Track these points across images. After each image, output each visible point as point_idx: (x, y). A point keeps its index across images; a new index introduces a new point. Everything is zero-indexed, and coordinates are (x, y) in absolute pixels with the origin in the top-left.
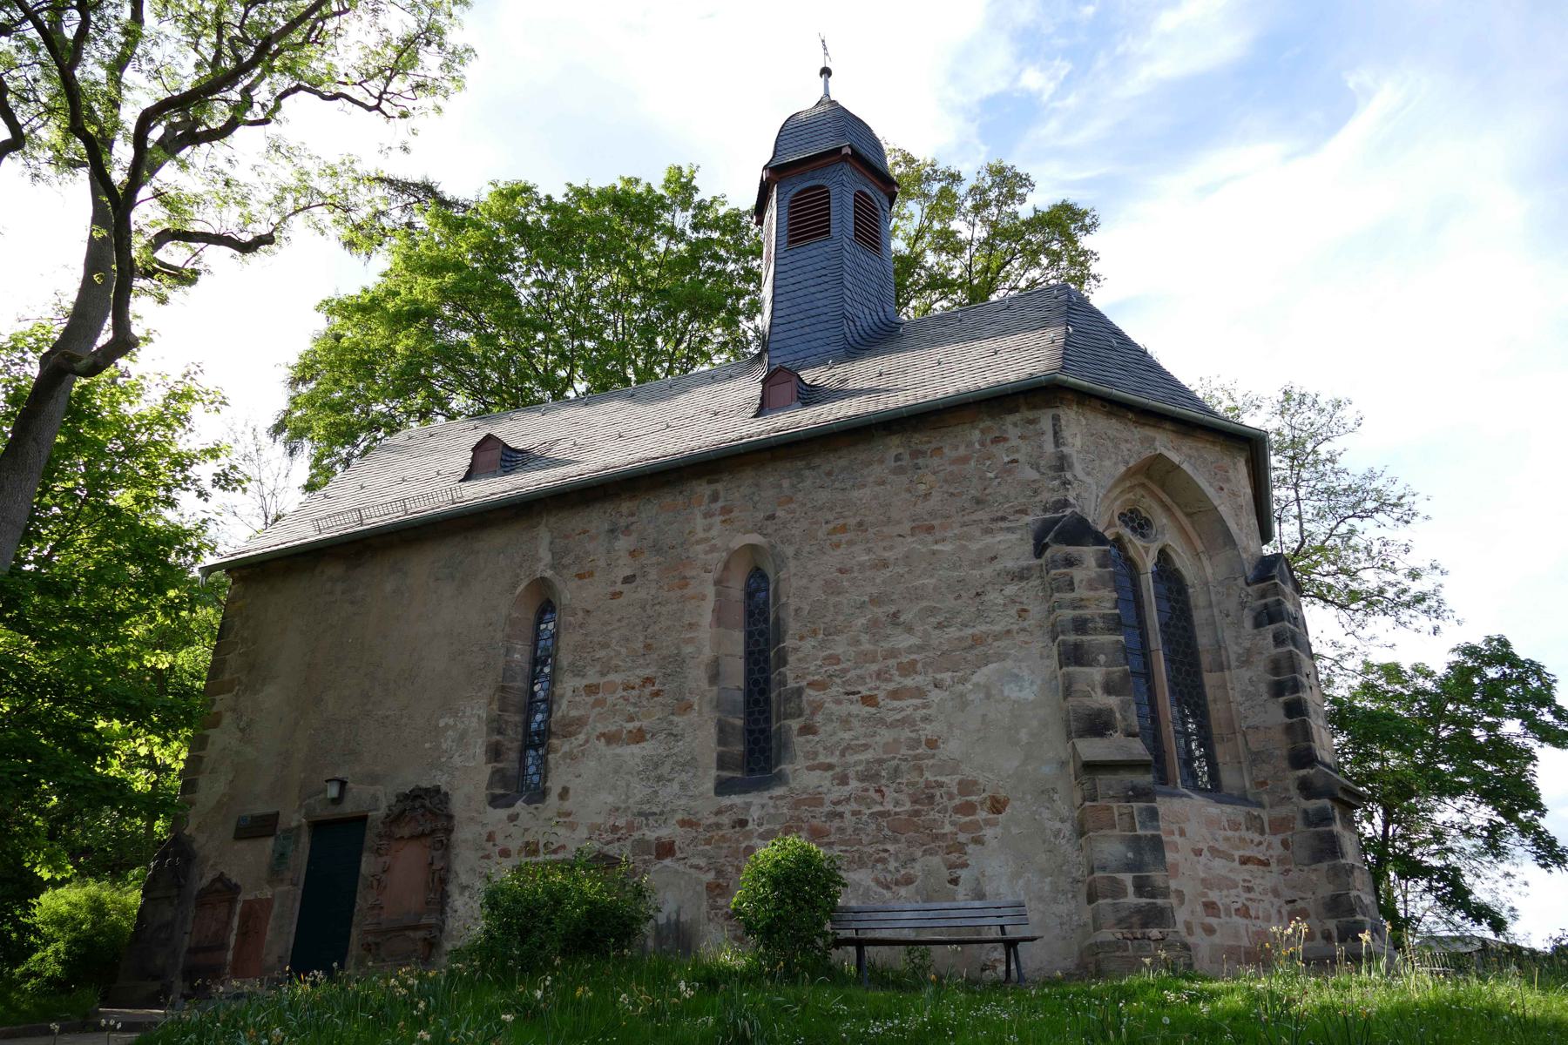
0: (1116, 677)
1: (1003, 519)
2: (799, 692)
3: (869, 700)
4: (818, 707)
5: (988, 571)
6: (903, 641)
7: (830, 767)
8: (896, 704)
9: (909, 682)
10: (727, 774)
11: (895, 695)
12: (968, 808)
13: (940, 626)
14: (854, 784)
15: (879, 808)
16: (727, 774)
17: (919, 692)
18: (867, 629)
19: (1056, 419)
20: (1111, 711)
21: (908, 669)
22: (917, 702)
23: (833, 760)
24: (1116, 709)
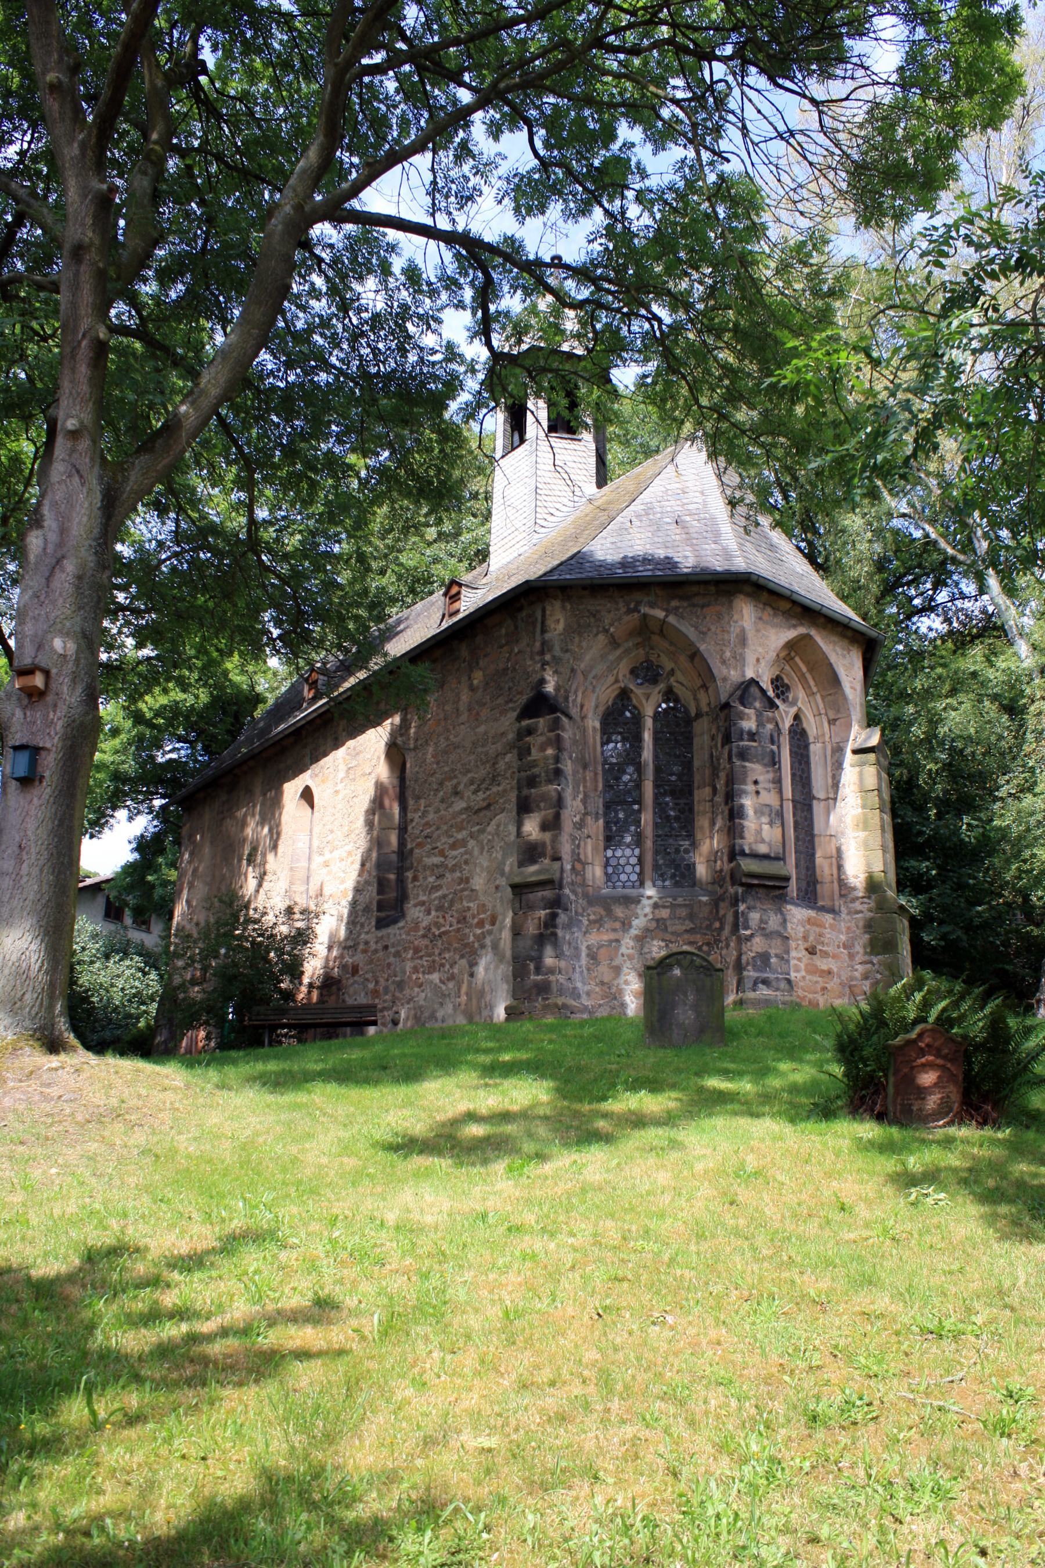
0: (550, 817)
1: (511, 701)
2: (412, 850)
3: (442, 853)
4: (420, 861)
5: (499, 747)
6: (460, 805)
7: (423, 903)
8: (454, 853)
9: (460, 836)
10: (383, 914)
11: (454, 846)
12: (481, 924)
13: (475, 792)
14: (433, 913)
15: (443, 929)
16: (383, 914)
17: (463, 843)
18: (442, 801)
19: (544, 611)
20: (544, 844)
21: (460, 829)
22: (462, 850)
23: (424, 898)
24: (548, 843)
